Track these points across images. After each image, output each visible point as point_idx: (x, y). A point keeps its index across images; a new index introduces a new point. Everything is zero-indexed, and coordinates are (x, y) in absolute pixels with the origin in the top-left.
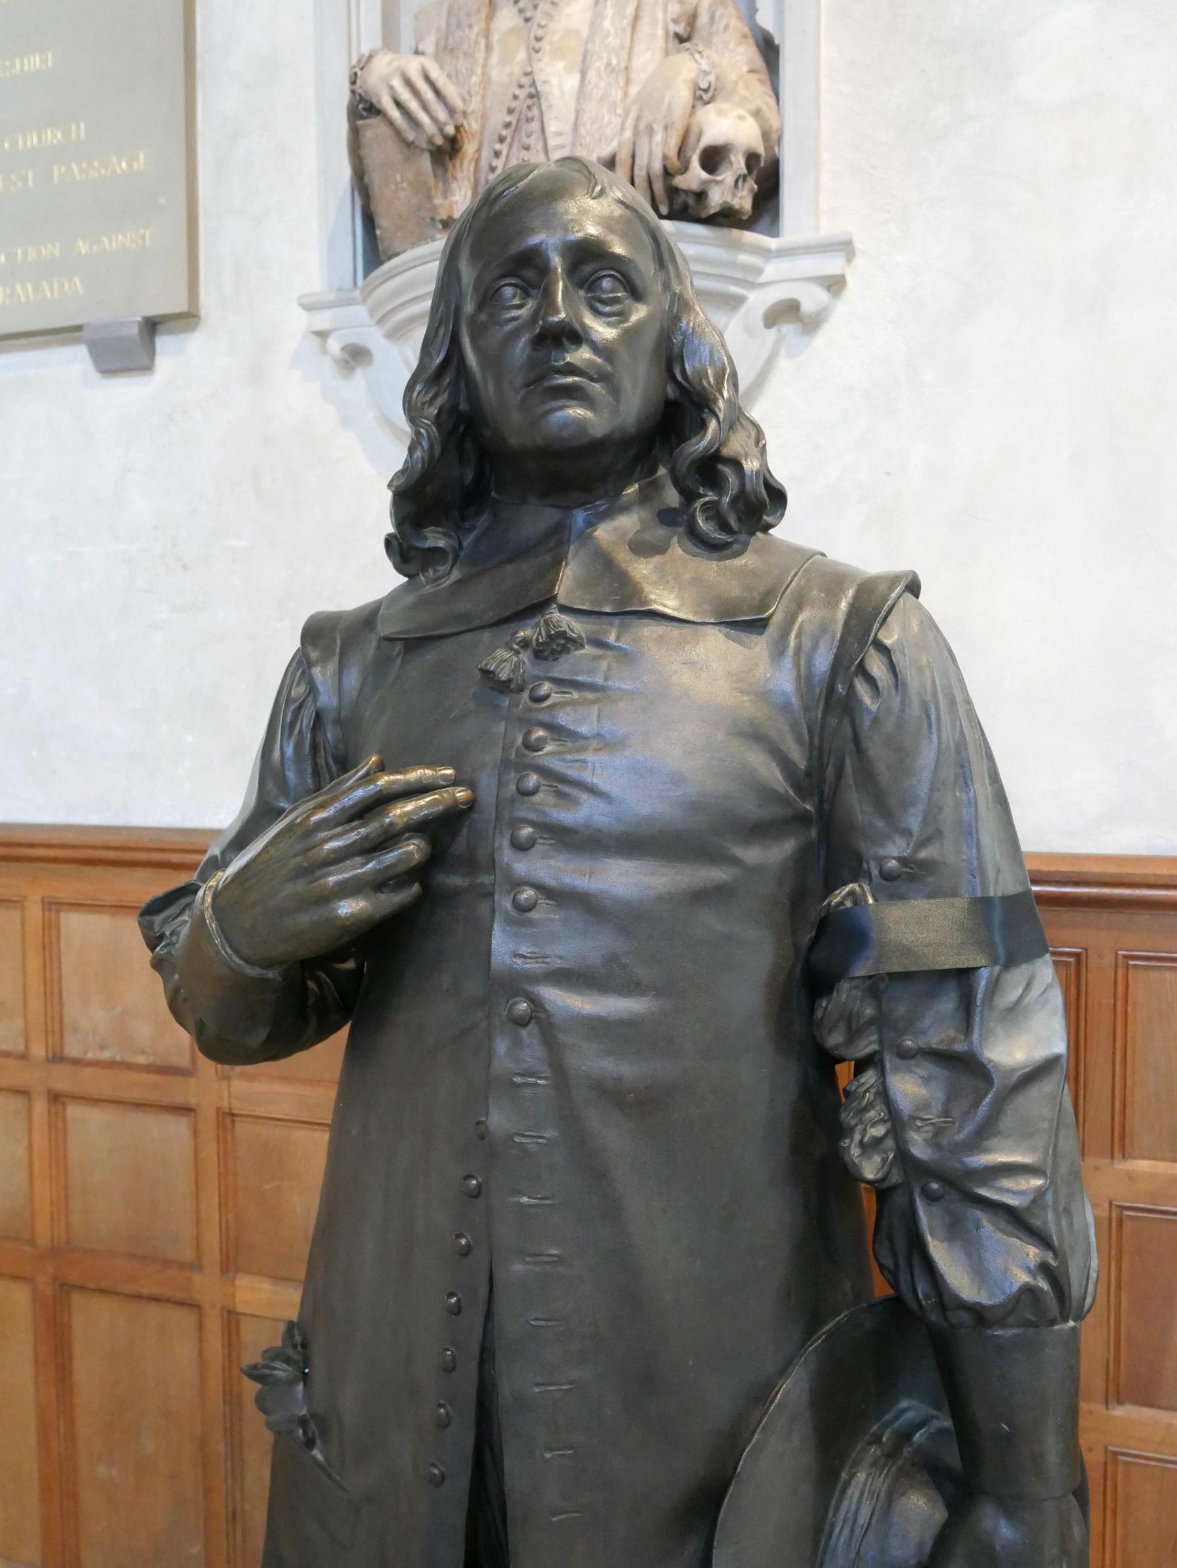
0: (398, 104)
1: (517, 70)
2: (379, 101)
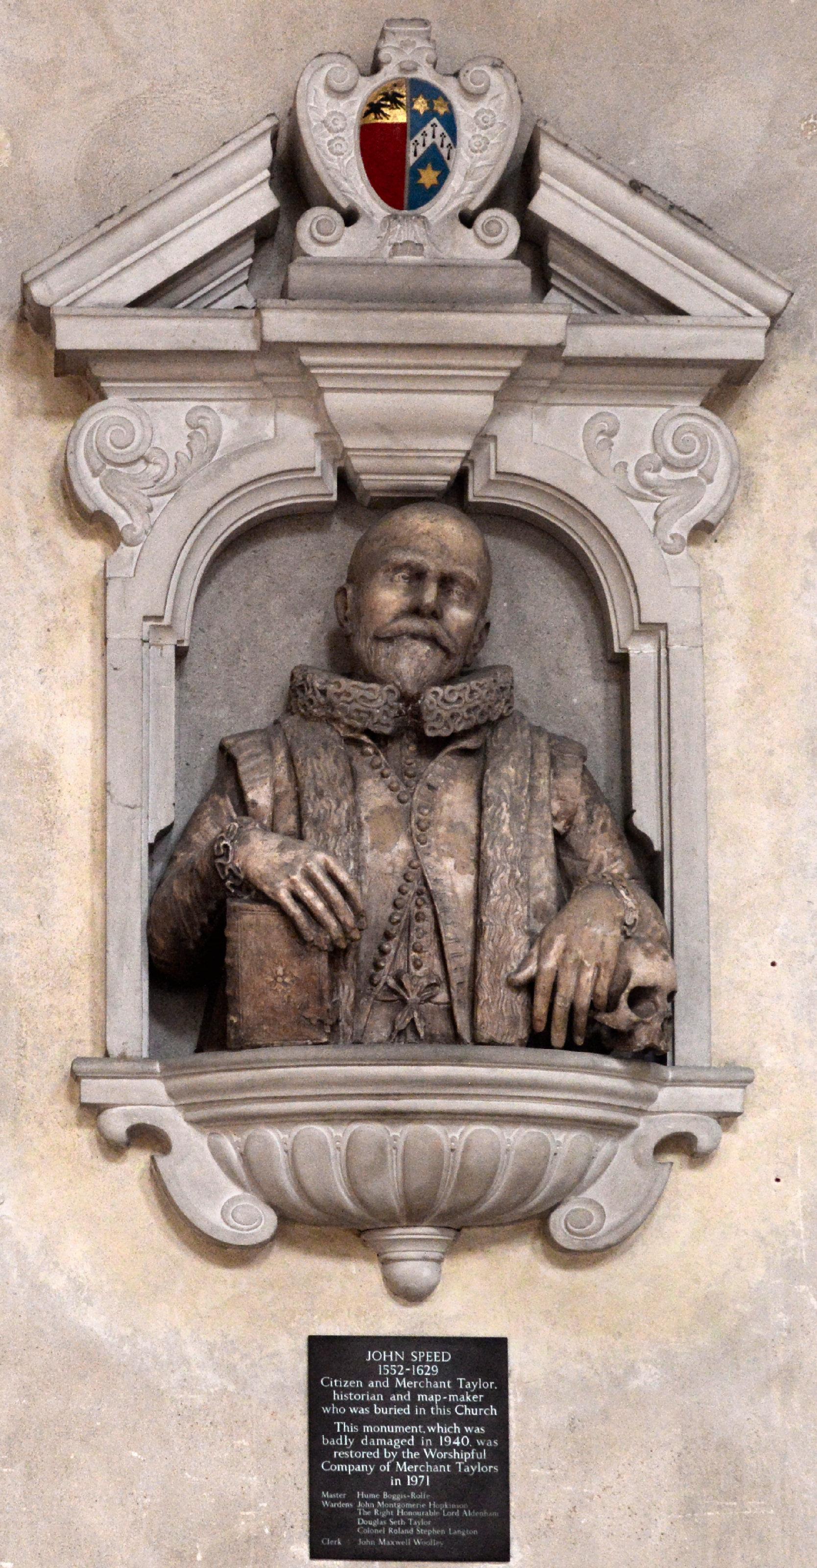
0: (297, 897)
1: (400, 862)
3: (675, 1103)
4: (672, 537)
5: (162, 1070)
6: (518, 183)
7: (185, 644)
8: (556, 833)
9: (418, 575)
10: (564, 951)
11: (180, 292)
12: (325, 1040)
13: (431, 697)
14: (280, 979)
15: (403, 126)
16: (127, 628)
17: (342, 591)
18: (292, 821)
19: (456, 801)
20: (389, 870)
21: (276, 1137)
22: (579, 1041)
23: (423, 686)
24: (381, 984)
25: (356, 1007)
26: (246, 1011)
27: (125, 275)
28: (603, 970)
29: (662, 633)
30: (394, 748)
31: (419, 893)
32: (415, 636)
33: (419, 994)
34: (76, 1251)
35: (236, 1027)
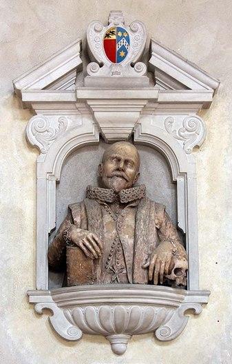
0: (84, 245)
1: (114, 236)
3: (188, 300)
6: (147, 55)
9: (119, 160)
11: (56, 86)
16: (42, 175)
17: (100, 165)
18: (85, 226)
19: (129, 220)
21: (80, 310)
22: (161, 283)
23: (120, 190)
25: (102, 275)
26: (71, 277)
30: (113, 206)
31: (119, 244)
34: (28, 343)
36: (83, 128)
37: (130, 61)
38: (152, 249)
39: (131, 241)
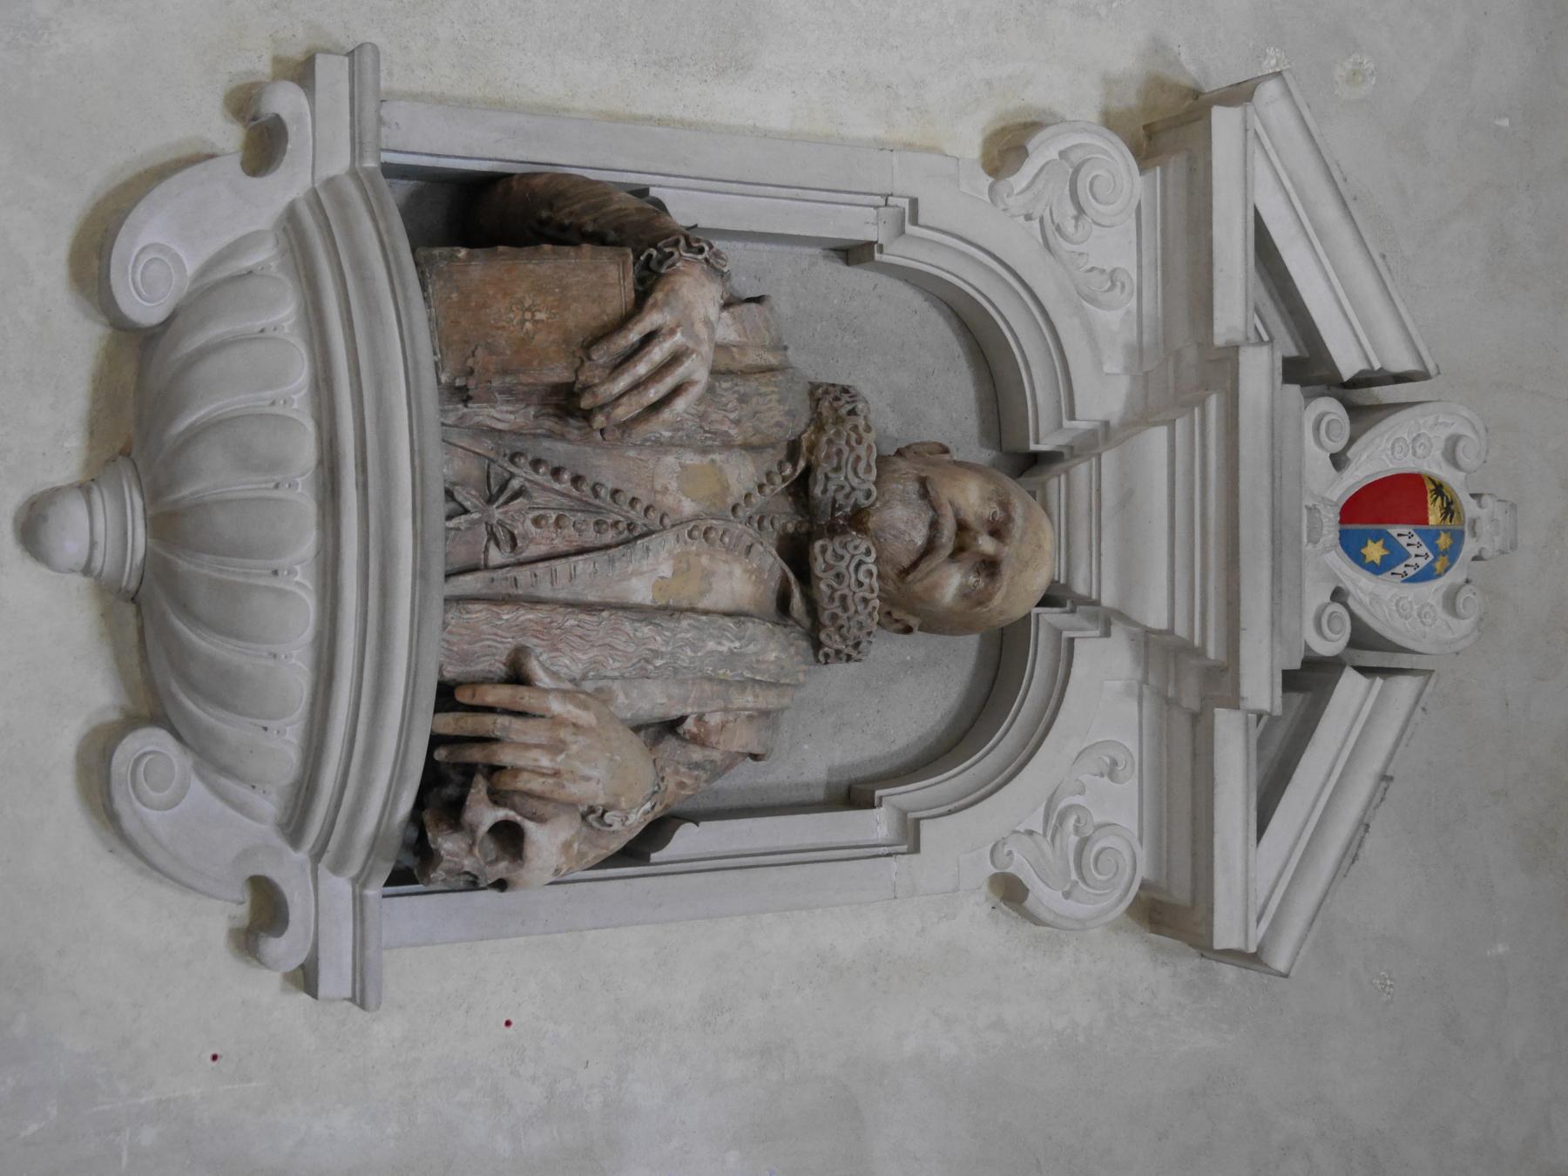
1: (669, 501)
2: (654, 305)
3: (325, 903)
4: (1010, 853)
5: (366, 169)
7: (877, 256)
8: (682, 719)
9: (998, 531)
10: (574, 725)
12: (444, 378)
13: (862, 549)
14: (528, 315)
15: (1425, 522)
16: (905, 179)
20: (658, 487)
21: (286, 313)
22: (441, 754)
24: (513, 469)
27: (1280, 197)
28: (551, 781)
29: (904, 848)
30: (786, 505)
31: (631, 526)
32: (934, 525)
33: (501, 524)
35: (452, 258)
36: (1091, 369)
37: (1347, 585)
38: (602, 697)
39: (641, 591)
